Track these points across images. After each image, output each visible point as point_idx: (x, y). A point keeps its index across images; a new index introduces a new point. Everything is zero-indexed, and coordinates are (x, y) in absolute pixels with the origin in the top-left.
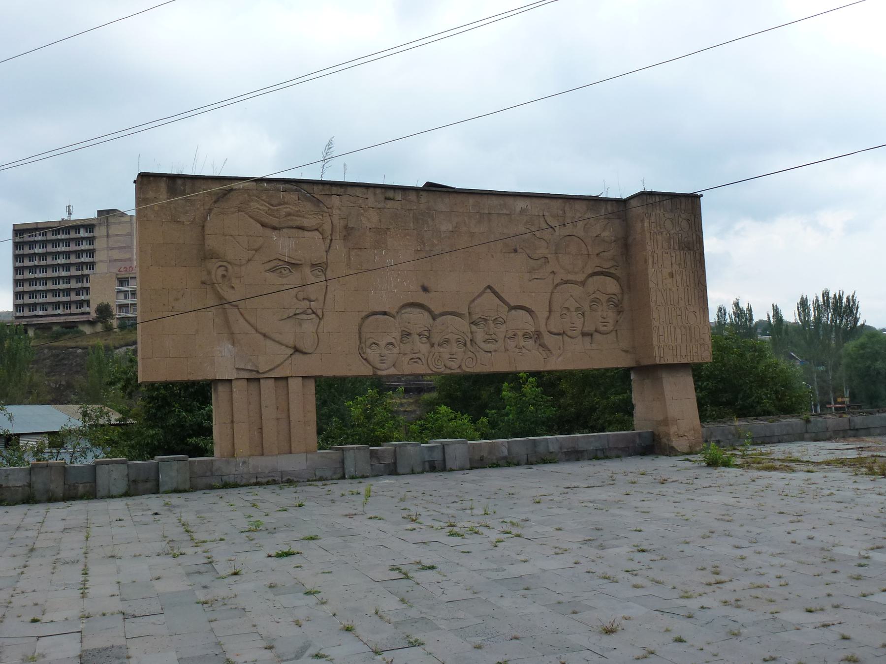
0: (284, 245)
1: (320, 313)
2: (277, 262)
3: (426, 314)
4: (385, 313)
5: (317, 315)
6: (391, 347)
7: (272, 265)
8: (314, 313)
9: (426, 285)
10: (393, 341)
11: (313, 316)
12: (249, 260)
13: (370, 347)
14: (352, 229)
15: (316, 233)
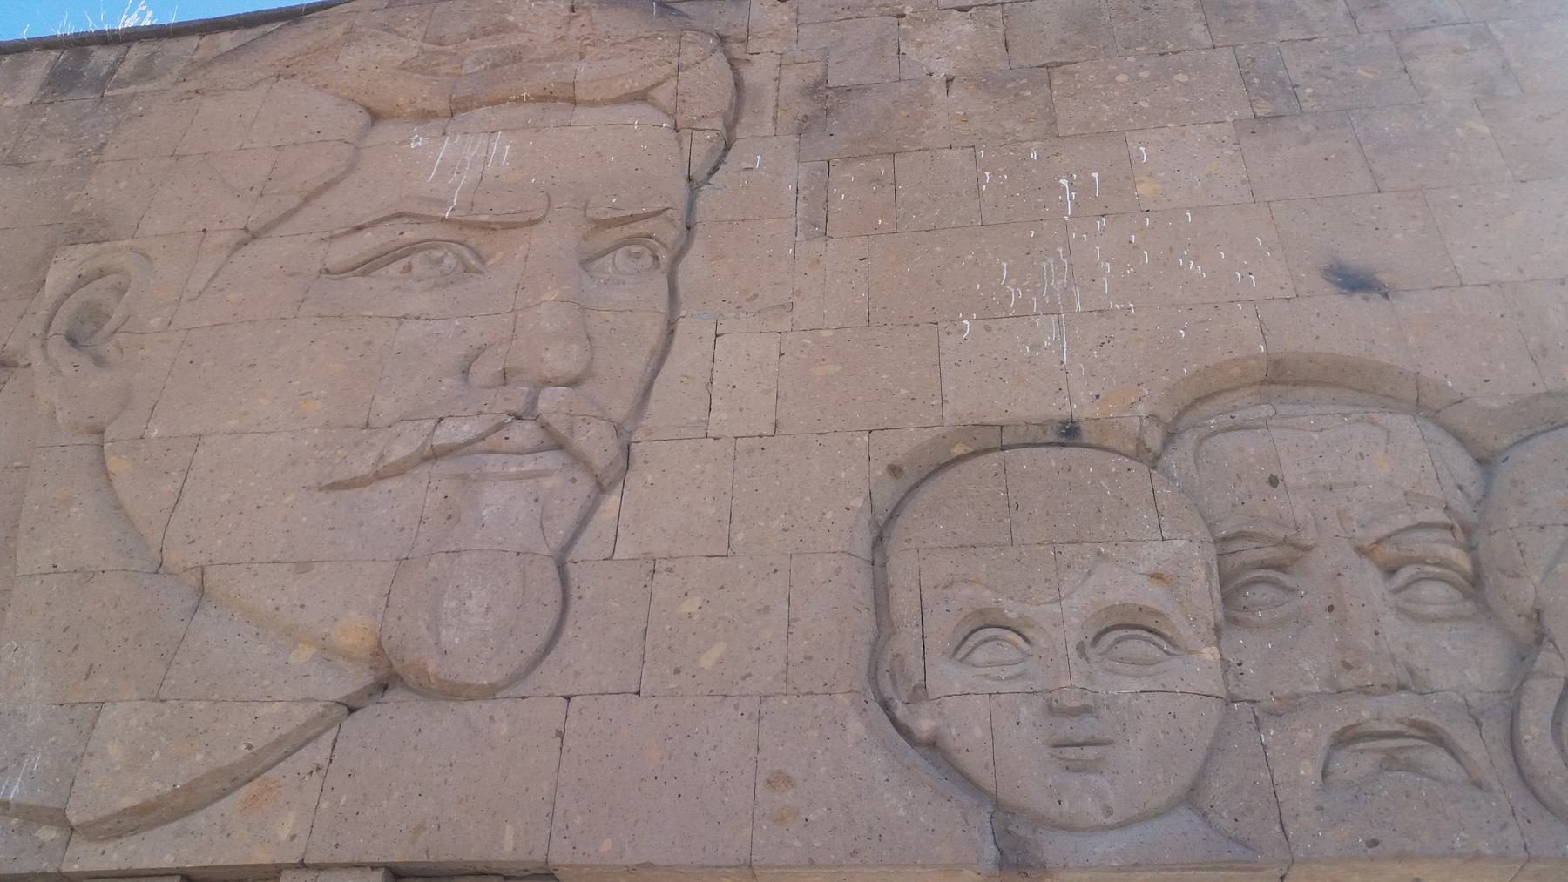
0: (461, 161)
1: (595, 441)
2: (398, 225)
3: (1402, 423)
4: (1070, 432)
5: (580, 460)
6: (1139, 647)
7: (369, 241)
8: (558, 444)
9: (1355, 254)
10: (1152, 596)
11: (550, 460)
12: (251, 236)
13: (959, 649)
14: (846, 90)
15: (642, 109)
